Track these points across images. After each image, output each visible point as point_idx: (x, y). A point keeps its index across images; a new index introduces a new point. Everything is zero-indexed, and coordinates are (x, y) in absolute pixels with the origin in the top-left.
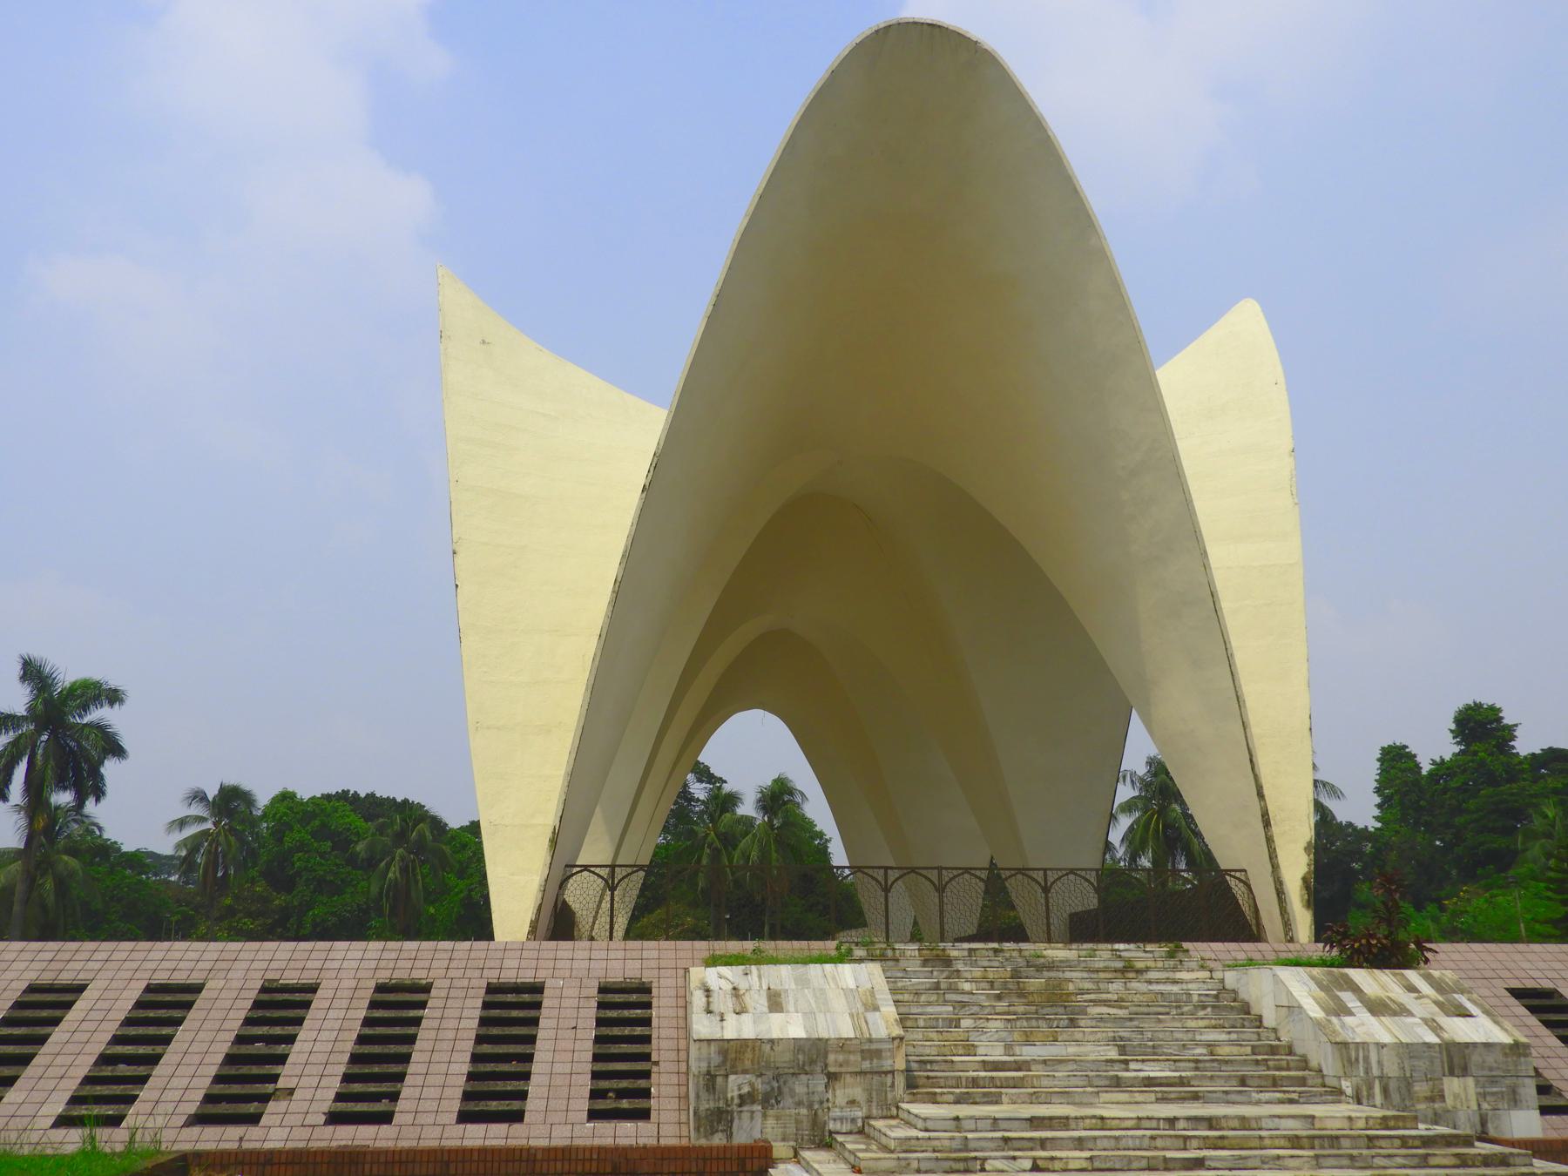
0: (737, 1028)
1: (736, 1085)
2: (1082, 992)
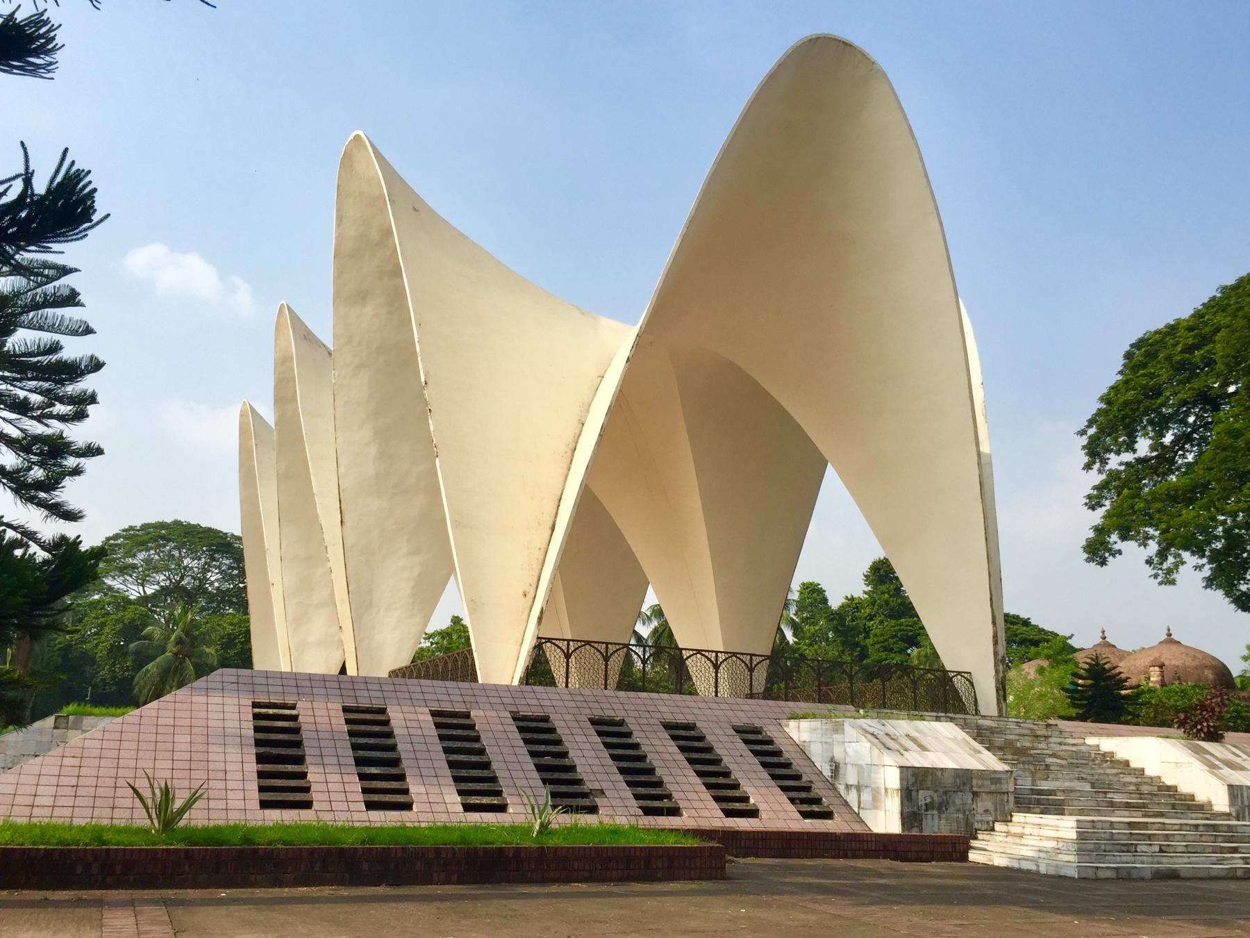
1: (923, 797)
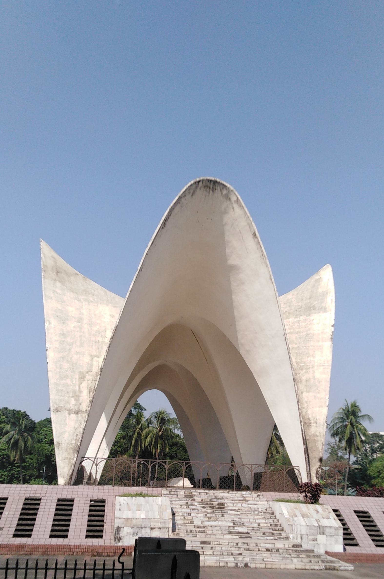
0: (128, 514)
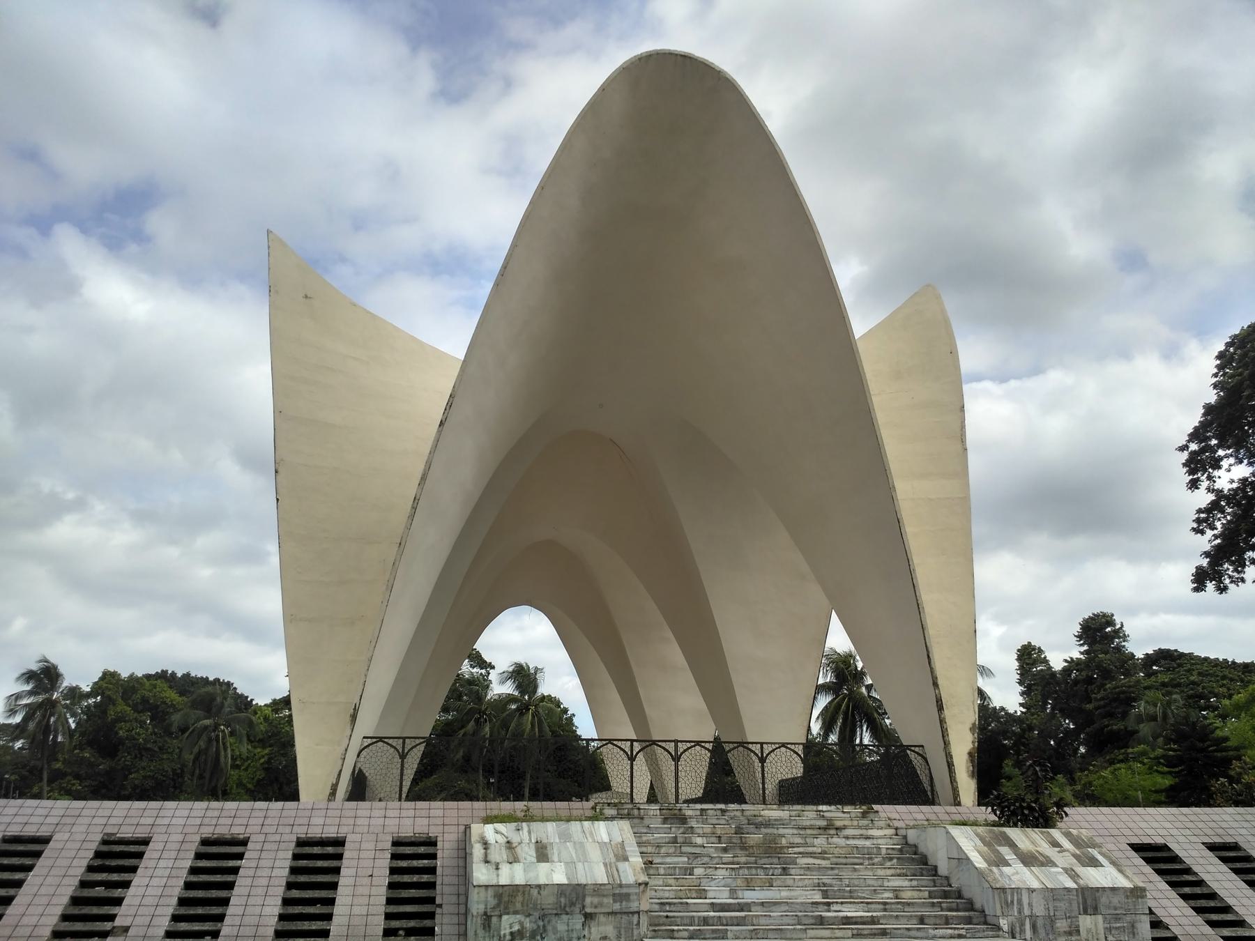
1: (508, 924)
2: (792, 845)
